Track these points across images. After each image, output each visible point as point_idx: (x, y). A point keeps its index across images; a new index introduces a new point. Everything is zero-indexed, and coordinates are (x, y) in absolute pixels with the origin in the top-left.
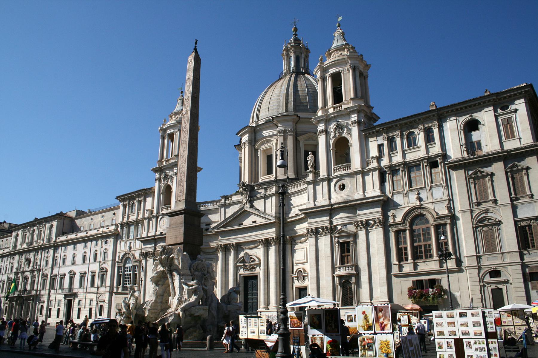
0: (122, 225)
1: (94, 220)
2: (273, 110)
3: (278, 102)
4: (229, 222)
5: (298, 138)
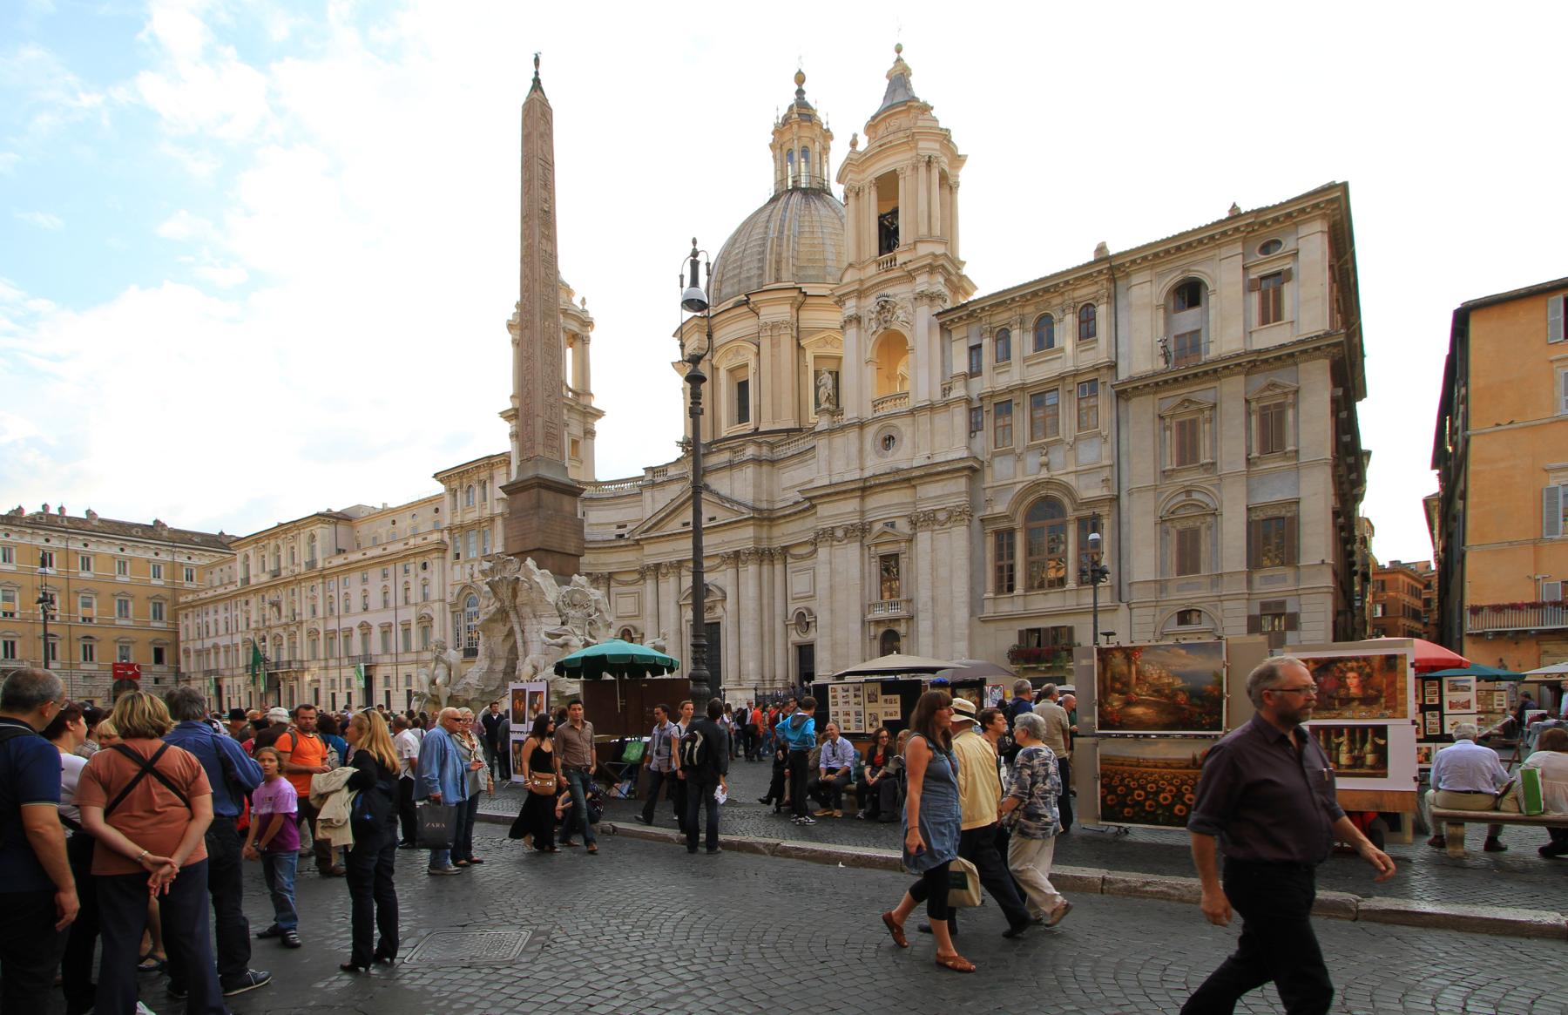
0: (450, 529)
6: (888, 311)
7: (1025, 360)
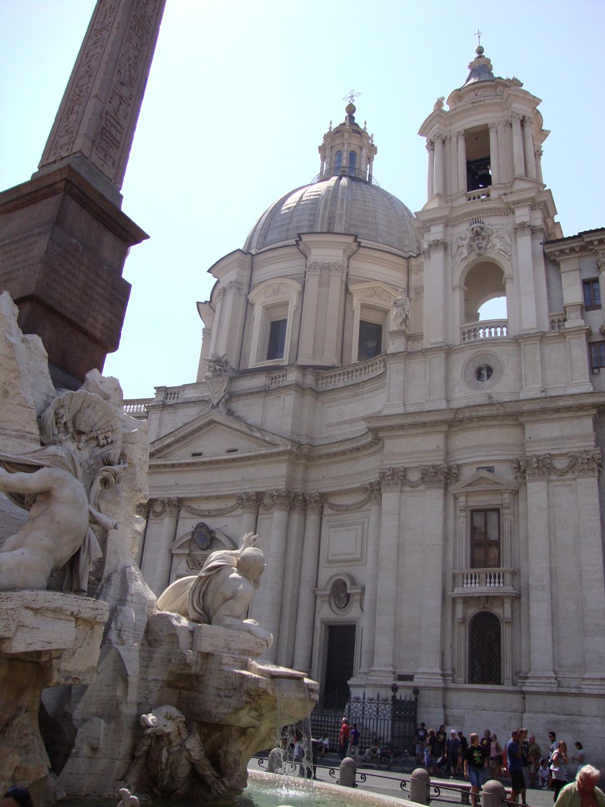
2: (298, 228)
3: (311, 214)
4: (169, 446)
6: (483, 239)
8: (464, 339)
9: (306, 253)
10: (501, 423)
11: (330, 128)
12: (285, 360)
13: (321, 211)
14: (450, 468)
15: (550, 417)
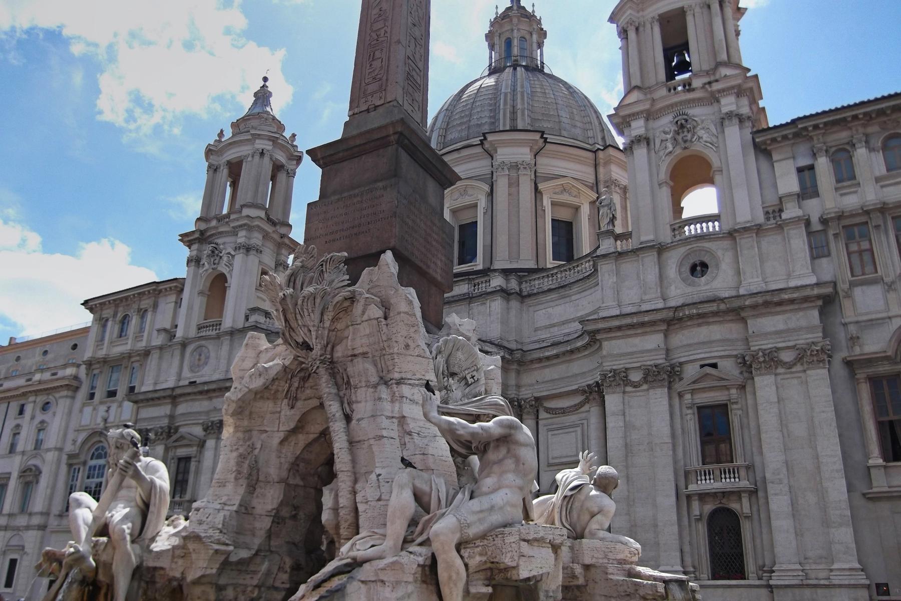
0: (89, 364)
1: (22, 362)
2: (479, 126)
5: (539, 185)
6: (688, 131)
7: (878, 180)
8: (674, 236)
9: (492, 152)
10: (722, 319)
11: (497, 13)
12: (479, 264)
13: (502, 107)
14: (673, 367)
15: (773, 310)
